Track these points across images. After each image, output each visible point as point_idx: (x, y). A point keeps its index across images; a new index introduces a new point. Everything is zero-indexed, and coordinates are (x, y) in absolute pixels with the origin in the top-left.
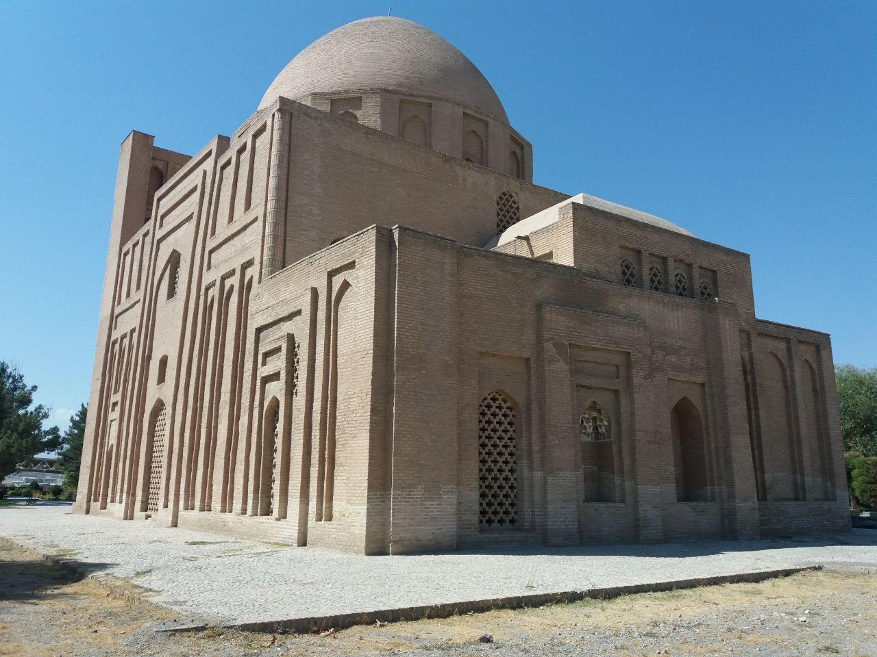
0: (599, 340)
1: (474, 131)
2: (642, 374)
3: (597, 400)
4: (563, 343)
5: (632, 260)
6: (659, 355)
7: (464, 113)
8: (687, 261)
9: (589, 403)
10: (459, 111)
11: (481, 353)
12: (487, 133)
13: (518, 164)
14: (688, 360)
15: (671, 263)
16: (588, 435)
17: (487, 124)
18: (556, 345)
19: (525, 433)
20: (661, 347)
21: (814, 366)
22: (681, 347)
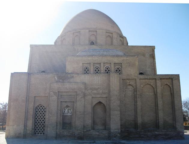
0: (67, 90)
1: (93, 34)
2: (80, 97)
3: (68, 105)
4: (56, 92)
5: (88, 66)
6: (90, 91)
7: (89, 31)
8: (109, 62)
9: (65, 106)
10: (88, 30)
11: (35, 97)
12: (97, 34)
13: (111, 38)
14: (101, 91)
15: (102, 65)
16: (70, 113)
17: (96, 31)
18: (54, 92)
19: (34, 113)
20: (91, 89)
21: (171, 86)
22: (98, 88)
